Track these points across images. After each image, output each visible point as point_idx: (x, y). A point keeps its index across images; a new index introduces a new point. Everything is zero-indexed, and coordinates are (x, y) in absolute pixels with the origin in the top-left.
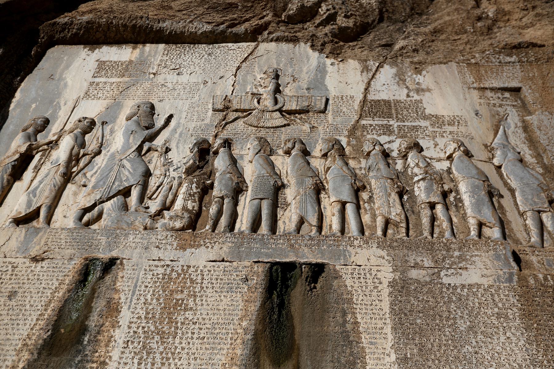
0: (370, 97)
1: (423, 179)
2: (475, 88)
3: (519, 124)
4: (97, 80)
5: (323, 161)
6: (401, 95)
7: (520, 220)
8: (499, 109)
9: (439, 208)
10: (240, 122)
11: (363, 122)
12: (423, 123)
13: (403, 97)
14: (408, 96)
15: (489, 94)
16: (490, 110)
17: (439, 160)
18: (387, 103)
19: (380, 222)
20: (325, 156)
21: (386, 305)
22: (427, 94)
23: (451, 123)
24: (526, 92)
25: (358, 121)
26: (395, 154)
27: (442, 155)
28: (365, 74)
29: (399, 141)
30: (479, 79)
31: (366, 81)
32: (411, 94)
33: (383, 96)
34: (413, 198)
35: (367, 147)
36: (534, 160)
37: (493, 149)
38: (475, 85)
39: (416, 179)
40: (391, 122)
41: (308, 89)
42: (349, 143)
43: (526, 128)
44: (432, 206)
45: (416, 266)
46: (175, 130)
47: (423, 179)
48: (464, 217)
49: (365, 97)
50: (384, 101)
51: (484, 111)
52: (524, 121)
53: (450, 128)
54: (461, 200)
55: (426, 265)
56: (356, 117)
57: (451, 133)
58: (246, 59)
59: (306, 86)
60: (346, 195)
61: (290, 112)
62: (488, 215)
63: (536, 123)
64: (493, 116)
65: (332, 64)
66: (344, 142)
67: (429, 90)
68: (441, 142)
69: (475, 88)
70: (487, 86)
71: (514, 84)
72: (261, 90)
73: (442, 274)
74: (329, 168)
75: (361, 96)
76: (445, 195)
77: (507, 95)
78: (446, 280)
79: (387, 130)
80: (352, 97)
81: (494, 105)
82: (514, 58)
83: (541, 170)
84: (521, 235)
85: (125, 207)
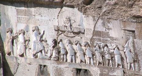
1: (108, 54)
2: (123, 30)
3: (132, 41)
5: (85, 47)
6: (104, 30)
7: (127, 65)
8: (128, 37)
10: (63, 35)
11: (94, 37)
12: (109, 39)
13: (104, 31)
14: (105, 30)
15: (126, 32)
16: (126, 37)
17: (112, 49)
18: (100, 32)
20: (85, 46)
22: (111, 30)
23: (115, 40)
25: (92, 37)
26: (101, 47)
27: (112, 48)
28: (94, 21)
29: (103, 43)
30: (125, 27)
31: (94, 24)
32: (106, 30)
33: (99, 30)
34: (105, 58)
35: (95, 44)
36: (133, 51)
37: (124, 48)
38: (123, 29)
39: (106, 53)
40: (101, 38)
41: (79, 25)
42: (90, 43)
43: (133, 43)
44: (109, 60)
45: (105, 71)
46: (46, 35)
47: (108, 54)
48: (115, 63)
49: (94, 29)
50: (99, 31)
51: (124, 37)
52: (133, 41)
53: (115, 41)
54: (115, 59)
55: (107, 71)
56: (92, 36)
57: (115, 42)
58: (60, 12)
59: (78, 25)
60: (91, 56)
62: (120, 63)
63: (136, 42)
64: (126, 38)
65: (85, 17)
66: (89, 42)
67: (111, 29)
68: (113, 45)
69: (123, 30)
70: (126, 29)
71: (133, 29)
72: (67, 25)
73: (109, 73)
74: (86, 49)
76: (112, 58)
77: (131, 32)
78: (110, 74)
79: (100, 40)
80: (91, 29)
81: (127, 35)
82: (135, 21)
83: (134, 54)
84: (126, 68)
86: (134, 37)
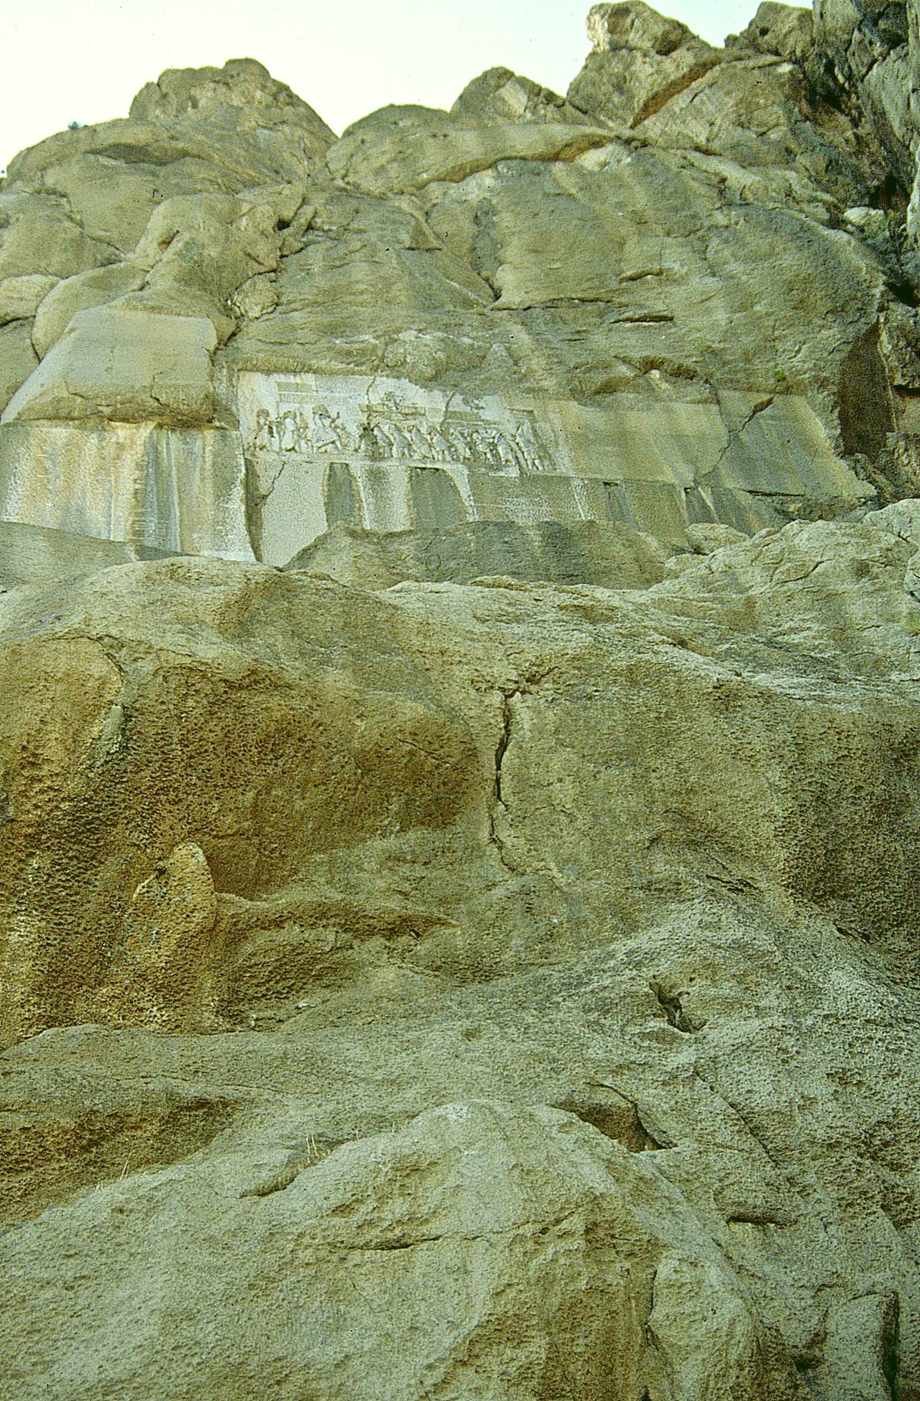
0: (450, 409)
4: (283, 393)
9: (489, 455)
19: (461, 458)
21: (467, 480)
24: (535, 412)
26: (466, 435)
30: (510, 403)
43: (533, 428)
51: (512, 419)
56: (443, 418)
61: (407, 414)
71: (530, 409)
75: (444, 409)
76: (491, 451)
84: (525, 466)
85: (337, 447)
86: (534, 421)
